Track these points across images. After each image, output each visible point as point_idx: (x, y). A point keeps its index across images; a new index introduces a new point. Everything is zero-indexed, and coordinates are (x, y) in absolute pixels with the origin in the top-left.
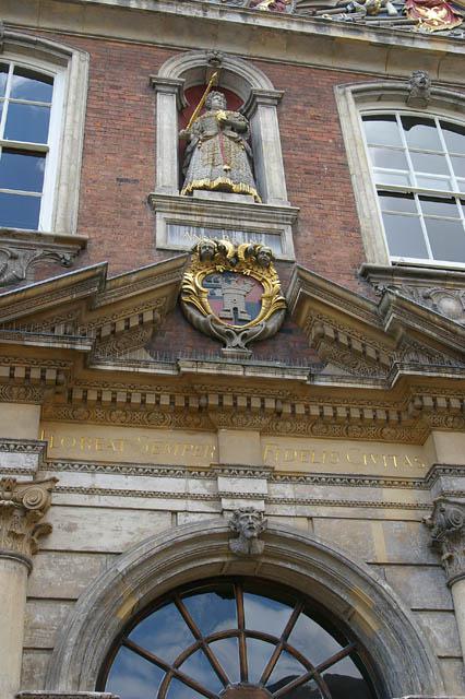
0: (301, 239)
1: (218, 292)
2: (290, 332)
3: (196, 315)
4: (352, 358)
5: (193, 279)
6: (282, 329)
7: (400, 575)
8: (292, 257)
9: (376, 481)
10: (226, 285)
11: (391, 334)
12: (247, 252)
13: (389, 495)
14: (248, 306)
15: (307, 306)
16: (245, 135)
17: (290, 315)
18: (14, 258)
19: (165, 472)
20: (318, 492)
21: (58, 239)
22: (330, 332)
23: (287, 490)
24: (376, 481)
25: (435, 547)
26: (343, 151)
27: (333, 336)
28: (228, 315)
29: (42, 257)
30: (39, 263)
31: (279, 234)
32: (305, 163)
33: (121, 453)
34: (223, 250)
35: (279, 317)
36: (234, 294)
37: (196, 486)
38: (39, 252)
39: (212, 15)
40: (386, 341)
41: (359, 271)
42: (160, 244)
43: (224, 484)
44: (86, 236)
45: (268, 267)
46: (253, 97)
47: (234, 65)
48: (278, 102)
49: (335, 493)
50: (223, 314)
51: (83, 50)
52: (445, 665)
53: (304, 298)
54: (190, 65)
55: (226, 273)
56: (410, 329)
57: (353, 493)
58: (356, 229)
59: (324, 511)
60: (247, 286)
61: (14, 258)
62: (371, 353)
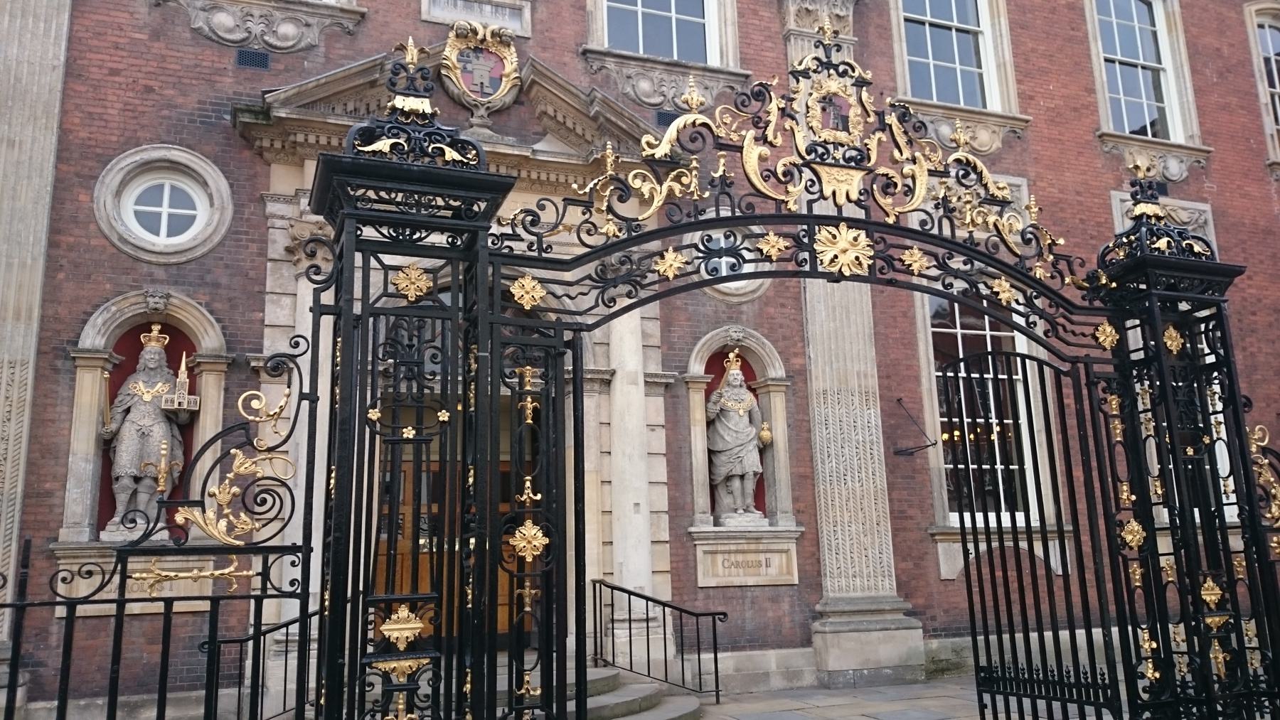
0: (538, 16)
1: (469, 67)
2: (522, 103)
3: (452, 87)
4: (564, 131)
5: (451, 53)
6: (517, 101)
8: (528, 34)
10: (475, 61)
11: (595, 119)
12: (493, 34)
14: (491, 79)
15: (535, 88)
17: (523, 92)
18: (308, 25)
21: (342, 10)
22: (551, 111)
27: (552, 114)
28: (478, 88)
29: (331, 25)
30: (328, 31)
31: (520, 9)
34: (475, 32)
35: (515, 91)
36: (482, 68)
38: (328, 21)
40: (590, 122)
41: (581, 50)
42: (424, 17)
44: (365, 10)
45: (509, 46)
50: (473, 88)
52: (597, 348)
53: (533, 82)
55: (477, 50)
56: (608, 120)
60: (492, 62)
61: (308, 25)
62: (579, 130)
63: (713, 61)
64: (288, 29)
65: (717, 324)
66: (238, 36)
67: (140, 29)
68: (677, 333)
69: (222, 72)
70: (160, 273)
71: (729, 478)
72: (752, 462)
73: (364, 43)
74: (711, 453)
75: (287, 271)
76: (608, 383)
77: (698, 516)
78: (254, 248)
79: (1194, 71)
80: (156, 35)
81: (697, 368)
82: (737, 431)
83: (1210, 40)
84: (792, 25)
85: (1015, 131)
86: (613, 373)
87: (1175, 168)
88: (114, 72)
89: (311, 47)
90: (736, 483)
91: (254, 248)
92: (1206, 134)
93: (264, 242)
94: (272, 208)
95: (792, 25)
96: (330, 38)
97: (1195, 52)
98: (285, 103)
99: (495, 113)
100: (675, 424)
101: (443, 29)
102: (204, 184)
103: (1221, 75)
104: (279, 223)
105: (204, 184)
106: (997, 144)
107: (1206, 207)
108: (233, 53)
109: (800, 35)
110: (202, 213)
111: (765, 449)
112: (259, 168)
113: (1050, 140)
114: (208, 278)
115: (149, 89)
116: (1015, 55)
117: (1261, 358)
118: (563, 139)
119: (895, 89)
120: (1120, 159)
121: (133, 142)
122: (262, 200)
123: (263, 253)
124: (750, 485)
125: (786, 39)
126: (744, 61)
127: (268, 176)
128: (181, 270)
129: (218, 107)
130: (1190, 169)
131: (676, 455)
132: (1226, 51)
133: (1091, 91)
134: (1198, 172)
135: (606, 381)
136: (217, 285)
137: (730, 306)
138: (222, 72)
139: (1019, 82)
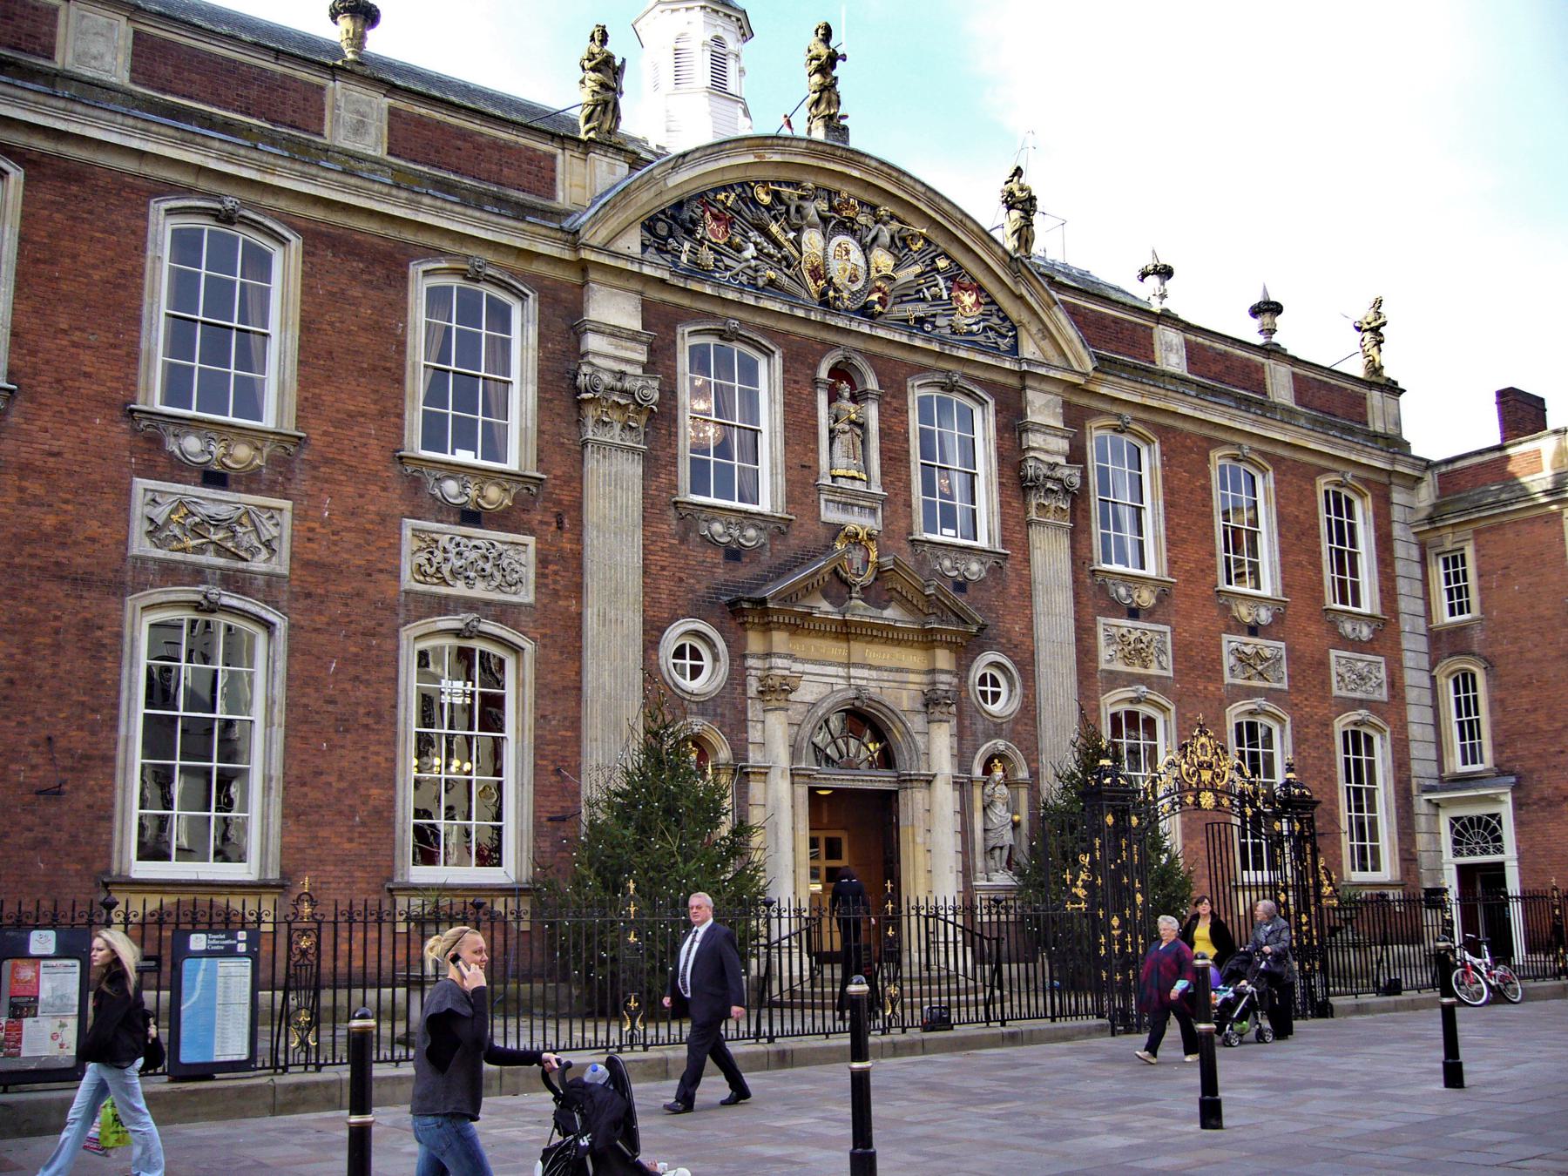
4: (904, 602)
7: (911, 716)
9: (908, 671)
13: (912, 677)
16: (862, 426)
19: (831, 664)
20: (885, 675)
23: (874, 674)
24: (908, 671)
25: (926, 706)
26: (907, 440)
32: (890, 451)
33: (813, 654)
36: (857, 556)
37: (842, 671)
39: (854, 326)
43: (853, 672)
46: (866, 392)
47: (858, 361)
48: (880, 398)
49: (892, 676)
51: (779, 345)
54: (832, 362)
57: (898, 676)
58: (910, 506)
59: (887, 684)
63: (982, 542)
64: (751, 533)
65: (988, 738)
66: (725, 540)
67: (673, 536)
68: (968, 743)
69: (715, 565)
70: (694, 707)
71: (994, 848)
72: (1008, 837)
73: (792, 541)
74: (986, 830)
75: (759, 706)
76: (929, 782)
77: (979, 875)
78: (739, 689)
79: (1280, 535)
80: (683, 540)
81: (978, 771)
82: (1000, 814)
83: (1292, 509)
84: (1033, 515)
85: (1164, 593)
86: (934, 776)
87: (1264, 616)
88: (663, 568)
89: (764, 545)
90: (997, 852)
91: (739, 689)
92: (1287, 587)
93: (744, 685)
94: (750, 662)
95: (1033, 515)
96: (772, 537)
97: (1282, 520)
98: (772, 599)
99: (863, 588)
100: (965, 812)
101: (836, 530)
102: (711, 645)
103: (1298, 537)
104: (754, 672)
105: (711, 645)
106: (1153, 601)
107: (1282, 645)
108: (722, 551)
109: (1039, 523)
110: (707, 662)
111: (1016, 826)
112: (740, 633)
113: (1186, 595)
114: (719, 711)
115: (681, 580)
116: (1167, 529)
117: (1310, 761)
118: (902, 606)
119: (1091, 559)
120: (1229, 608)
121: (674, 618)
122: (744, 657)
123: (744, 692)
124: (1006, 852)
125: (1029, 524)
126: (1004, 542)
127: (745, 638)
128: (706, 706)
129: (718, 591)
130: (1274, 615)
131: (965, 832)
132: (1302, 517)
133: (1213, 555)
134: (1278, 618)
135: (929, 781)
136: (723, 715)
137: (996, 725)
138: (715, 565)
139: (1168, 550)
